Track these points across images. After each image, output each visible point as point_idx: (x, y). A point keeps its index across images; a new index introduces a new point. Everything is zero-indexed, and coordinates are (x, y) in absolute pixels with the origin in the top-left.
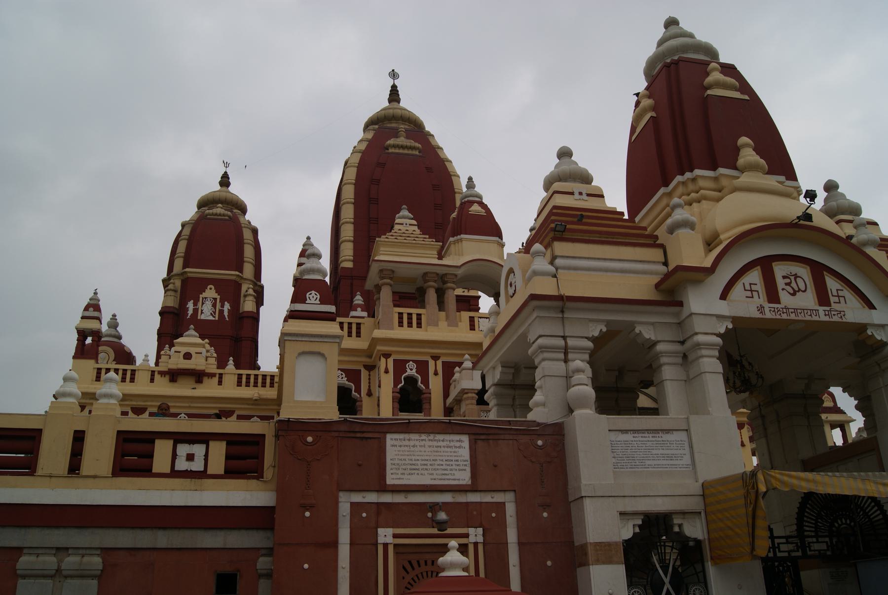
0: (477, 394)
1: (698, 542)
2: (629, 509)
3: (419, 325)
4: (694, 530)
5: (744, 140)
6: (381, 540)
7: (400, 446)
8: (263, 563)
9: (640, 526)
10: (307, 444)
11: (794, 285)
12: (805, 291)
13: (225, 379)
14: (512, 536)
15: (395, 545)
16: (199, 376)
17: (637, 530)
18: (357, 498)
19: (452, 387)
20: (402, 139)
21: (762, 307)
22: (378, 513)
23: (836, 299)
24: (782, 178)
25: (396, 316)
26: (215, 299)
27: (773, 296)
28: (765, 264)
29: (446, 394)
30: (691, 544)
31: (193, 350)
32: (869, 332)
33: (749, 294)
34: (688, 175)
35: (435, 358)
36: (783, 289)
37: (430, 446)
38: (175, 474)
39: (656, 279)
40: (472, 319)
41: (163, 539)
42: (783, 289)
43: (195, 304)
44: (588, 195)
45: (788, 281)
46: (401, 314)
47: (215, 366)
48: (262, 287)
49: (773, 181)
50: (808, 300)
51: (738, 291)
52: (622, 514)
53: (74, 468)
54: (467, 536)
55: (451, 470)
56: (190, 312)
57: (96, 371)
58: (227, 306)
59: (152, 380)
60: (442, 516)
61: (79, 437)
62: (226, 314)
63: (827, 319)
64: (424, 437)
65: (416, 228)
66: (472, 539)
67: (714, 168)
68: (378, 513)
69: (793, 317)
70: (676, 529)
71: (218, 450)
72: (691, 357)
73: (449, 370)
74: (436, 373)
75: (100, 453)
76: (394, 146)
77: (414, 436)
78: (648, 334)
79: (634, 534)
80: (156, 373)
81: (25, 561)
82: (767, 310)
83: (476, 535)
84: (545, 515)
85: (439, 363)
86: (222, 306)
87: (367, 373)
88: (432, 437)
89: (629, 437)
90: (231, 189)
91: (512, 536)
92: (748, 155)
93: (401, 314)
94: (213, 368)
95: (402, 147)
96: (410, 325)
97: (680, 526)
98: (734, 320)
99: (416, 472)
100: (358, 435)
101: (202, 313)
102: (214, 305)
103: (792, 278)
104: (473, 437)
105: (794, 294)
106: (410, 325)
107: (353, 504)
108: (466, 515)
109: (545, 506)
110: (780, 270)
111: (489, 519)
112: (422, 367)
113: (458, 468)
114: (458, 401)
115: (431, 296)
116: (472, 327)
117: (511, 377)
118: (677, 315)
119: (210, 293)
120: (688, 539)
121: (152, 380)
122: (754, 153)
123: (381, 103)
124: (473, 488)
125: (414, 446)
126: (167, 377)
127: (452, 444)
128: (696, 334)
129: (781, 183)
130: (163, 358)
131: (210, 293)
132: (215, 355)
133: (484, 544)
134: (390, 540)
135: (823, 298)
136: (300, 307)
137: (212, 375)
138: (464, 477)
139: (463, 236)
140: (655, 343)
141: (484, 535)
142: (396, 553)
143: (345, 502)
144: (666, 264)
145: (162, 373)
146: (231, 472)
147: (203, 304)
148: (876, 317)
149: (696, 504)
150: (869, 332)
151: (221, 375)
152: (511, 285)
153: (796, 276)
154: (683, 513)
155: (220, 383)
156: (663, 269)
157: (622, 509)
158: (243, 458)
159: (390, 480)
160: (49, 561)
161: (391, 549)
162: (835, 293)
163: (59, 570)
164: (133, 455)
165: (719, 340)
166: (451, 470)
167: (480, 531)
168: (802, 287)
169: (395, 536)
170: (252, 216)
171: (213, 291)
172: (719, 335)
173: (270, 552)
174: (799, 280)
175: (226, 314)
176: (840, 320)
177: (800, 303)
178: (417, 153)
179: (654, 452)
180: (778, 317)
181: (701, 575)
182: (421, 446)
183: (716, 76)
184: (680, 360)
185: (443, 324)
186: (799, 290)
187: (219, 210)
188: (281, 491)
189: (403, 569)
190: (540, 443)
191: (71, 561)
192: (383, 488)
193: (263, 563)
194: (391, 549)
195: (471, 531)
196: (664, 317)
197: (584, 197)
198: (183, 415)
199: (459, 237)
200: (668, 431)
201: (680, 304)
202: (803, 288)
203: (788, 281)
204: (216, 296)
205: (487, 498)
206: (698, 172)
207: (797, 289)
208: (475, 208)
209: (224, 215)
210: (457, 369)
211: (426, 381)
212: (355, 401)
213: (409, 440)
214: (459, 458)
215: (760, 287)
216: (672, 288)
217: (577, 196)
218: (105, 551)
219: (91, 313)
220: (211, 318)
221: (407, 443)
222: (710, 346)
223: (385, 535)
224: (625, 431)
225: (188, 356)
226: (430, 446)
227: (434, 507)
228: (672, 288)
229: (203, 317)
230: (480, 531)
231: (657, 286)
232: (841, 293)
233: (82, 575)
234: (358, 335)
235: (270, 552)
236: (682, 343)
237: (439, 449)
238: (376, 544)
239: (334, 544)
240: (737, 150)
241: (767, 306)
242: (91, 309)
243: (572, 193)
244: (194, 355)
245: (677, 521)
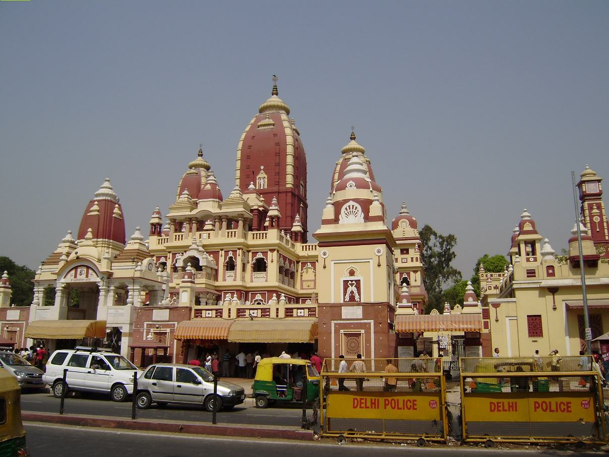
20: (267, 119)
27: (75, 277)
28: (76, 268)
40: (200, 235)
50: (84, 276)
51: (69, 275)
98: (67, 283)
108: (17, 325)
110: (79, 270)
135: (87, 276)
165: (61, 288)
187: (193, 171)
215: (74, 275)
222: (59, 290)
240: (86, 232)
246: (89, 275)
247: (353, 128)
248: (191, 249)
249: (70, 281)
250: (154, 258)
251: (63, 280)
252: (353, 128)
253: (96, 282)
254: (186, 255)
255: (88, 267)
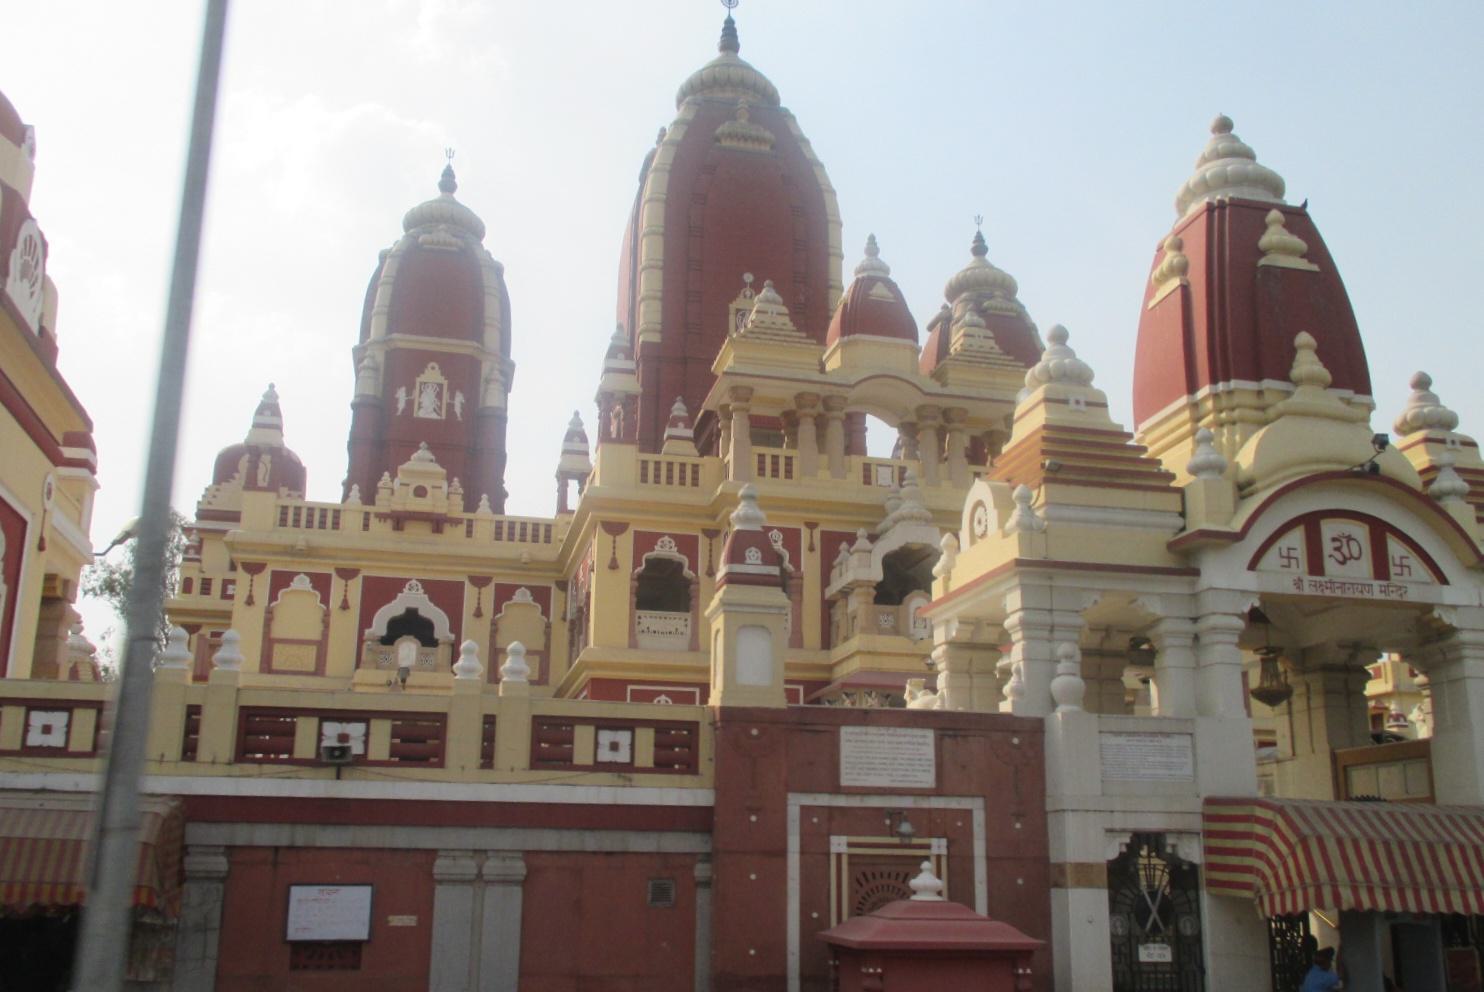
0: (875, 588)
1: (1193, 867)
2: (1118, 826)
3: (789, 474)
4: (1192, 852)
5: (1304, 338)
6: (834, 849)
7: (856, 741)
8: (701, 871)
9: (1127, 845)
10: (751, 737)
11: (1345, 550)
12: (1357, 559)
13: (477, 529)
14: (979, 848)
15: (851, 856)
16: (437, 523)
17: (1124, 849)
18: (809, 800)
19: (835, 573)
21: (1300, 580)
22: (830, 818)
23: (1398, 570)
24: (1348, 393)
25: (756, 459)
26: (440, 386)
27: (1316, 566)
28: (1310, 523)
29: (826, 581)
30: (1185, 867)
31: (427, 484)
32: (1436, 614)
33: (1285, 562)
34: (1221, 386)
35: (811, 525)
36: (1331, 556)
37: (889, 743)
38: (599, 767)
39: (1169, 536)
41: (591, 841)
42: (1331, 556)
43: (409, 392)
44: (1088, 404)
45: (1337, 544)
46: (762, 457)
47: (462, 508)
48: (512, 366)
49: (1333, 400)
50: (1363, 568)
51: (1271, 558)
52: (1110, 831)
53: (488, 759)
54: (928, 847)
55: (913, 770)
56: (401, 405)
57: (279, 510)
58: (459, 399)
59: (366, 526)
60: (906, 828)
61: (490, 721)
62: (458, 410)
63: (1382, 597)
64: (883, 730)
65: (786, 320)
66: (934, 851)
67: (1258, 377)
68: (830, 818)
69: (1338, 593)
70: (1169, 850)
71: (646, 738)
72: (1205, 640)
73: (832, 545)
74: (811, 549)
75: (514, 743)
76: (730, 136)
77: (872, 730)
78: (1155, 608)
79: (1121, 854)
80: (372, 516)
81: (441, 866)
82: (1306, 584)
83: (939, 846)
84: (1018, 826)
85: (817, 533)
86: (452, 397)
87: (707, 540)
88: (892, 730)
89: (1122, 740)
90: (458, 196)
91: (979, 848)
92: (1307, 363)
93: (762, 457)
94: (456, 508)
95: (745, 138)
96: (775, 473)
97: (1174, 846)
98: (1265, 597)
99: (872, 772)
100: (809, 727)
101: (420, 407)
102: (439, 396)
103: (1344, 541)
104: (940, 732)
105: (1343, 563)
106: (775, 473)
107: (803, 808)
108: (931, 823)
109: (1018, 816)
110: (1329, 529)
111: (955, 829)
112: (792, 538)
113: (921, 768)
114: (845, 593)
115: (807, 430)
116: (867, 480)
117: (969, 635)
118: (1193, 584)
119: (432, 375)
120: (1181, 862)
121: (366, 526)
122: (1316, 358)
123: (705, 53)
124: (938, 792)
125: (871, 742)
126: (389, 523)
127: (915, 740)
128: (1214, 614)
129: (1349, 402)
130: (382, 495)
131: (432, 375)
132: (461, 491)
133: (949, 857)
134: (844, 849)
135: (1381, 569)
136: (738, 568)
137: (456, 522)
138: (928, 780)
139: (857, 336)
140: (1158, 621)
141: (948, 847)
142: (850, 864)
143: (795, 802)
144: (1183, 514)
145: (382, 517)
146: (662, 765)
147: (421, 392)
148: (1449, 595)
149: (1197, 824)
150: (1436, 614)
151: (470, 523)
152: (980, 522)
153: (1349, 538)
154: (1180, 833)
155: (469, 533)
156: (1179, 522)
157: (1109, 826)
158: (675, 750)
159: (845, 781)
160: (468, 867)
161: (845, 860)
162: (1397, 562)
163: (480, 875)
164: (551, 744)
165: (1240, 624)
166: (913, 770)
167: (944, 842)
168: (1355, 553)
169: (850, 845)
170: (493, 245)
171: (437, 371)
172: (1241, 616)
173: (708, 857)
174: (1352, 543)
175: (458, 410)
176: (1398, 598)
177: (1352, 573)
178: (766, 148)
179: (1151, 759)
180: (1319, 593)
181: (1194, 905)
182: (880, 742)
183: (1275, 234)
184: (1189, 642)
185: (824, 474)
186: (1352, 557)
188: (719, 789)
189: (857, 882)
190: (1016, 741)
191: (492, 867)
192: (837, 789)
193: (701, 871)
194: (845, 860)
195: (934, 842)
196: (1177, 586)
197: (1083, 407)
198: (414, 582)
199: (851, 337)
200: (1168, 735)
201: (1196, 573)
202: (1356, 554)
203: (1337, 544)
204: (442, 380)
205: (954, 804)
206: (1233, 384)
207: (1347, 555)
208: (879, 291)
209: (450, 245)
210: (844, 546)
211: (796, 560)
212: (687, 583)
213: (866, 734)
214: (923, 757)
216: (1187, 555)
217: (1072, 406)
218: (528, 855)
219: (267, 419)
220: (434, 416)
221: (864, 738)
222: (1229, 630)
223: (839, 844)
224: (1118, 734)
225: (420, 492)
226: (889, 743)
227: (897, 815)
228: (1187, 555)
229: (421, 414)
230: (944, 842)
231: (1171, 546)
232: (1405, 562)
233: (506, 882)
234: (695, 482)
235: (708, 857)
236: (1195, 620)
237: (900, 746)
238: (828, 854)
239: (782, 853)
240: (1292, 352)
241: (1307, 579)
242: (268, 413)
243: (1065, 402)
244: (429, 489)
245: (1170, 840)
246: (1393, 570)
247: (979, 220)
248: (903, 518)
249: (1292, 590)
250: (626, 541)
251: (1250, 581)
252: (979, 220)
253: (1428, 608)
254: (891, 543)
255: (1379, 530)
